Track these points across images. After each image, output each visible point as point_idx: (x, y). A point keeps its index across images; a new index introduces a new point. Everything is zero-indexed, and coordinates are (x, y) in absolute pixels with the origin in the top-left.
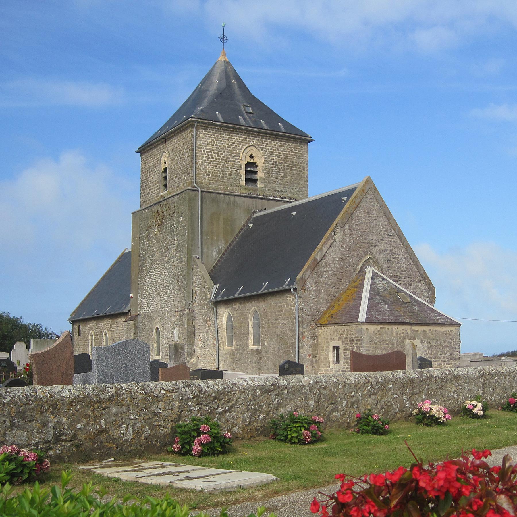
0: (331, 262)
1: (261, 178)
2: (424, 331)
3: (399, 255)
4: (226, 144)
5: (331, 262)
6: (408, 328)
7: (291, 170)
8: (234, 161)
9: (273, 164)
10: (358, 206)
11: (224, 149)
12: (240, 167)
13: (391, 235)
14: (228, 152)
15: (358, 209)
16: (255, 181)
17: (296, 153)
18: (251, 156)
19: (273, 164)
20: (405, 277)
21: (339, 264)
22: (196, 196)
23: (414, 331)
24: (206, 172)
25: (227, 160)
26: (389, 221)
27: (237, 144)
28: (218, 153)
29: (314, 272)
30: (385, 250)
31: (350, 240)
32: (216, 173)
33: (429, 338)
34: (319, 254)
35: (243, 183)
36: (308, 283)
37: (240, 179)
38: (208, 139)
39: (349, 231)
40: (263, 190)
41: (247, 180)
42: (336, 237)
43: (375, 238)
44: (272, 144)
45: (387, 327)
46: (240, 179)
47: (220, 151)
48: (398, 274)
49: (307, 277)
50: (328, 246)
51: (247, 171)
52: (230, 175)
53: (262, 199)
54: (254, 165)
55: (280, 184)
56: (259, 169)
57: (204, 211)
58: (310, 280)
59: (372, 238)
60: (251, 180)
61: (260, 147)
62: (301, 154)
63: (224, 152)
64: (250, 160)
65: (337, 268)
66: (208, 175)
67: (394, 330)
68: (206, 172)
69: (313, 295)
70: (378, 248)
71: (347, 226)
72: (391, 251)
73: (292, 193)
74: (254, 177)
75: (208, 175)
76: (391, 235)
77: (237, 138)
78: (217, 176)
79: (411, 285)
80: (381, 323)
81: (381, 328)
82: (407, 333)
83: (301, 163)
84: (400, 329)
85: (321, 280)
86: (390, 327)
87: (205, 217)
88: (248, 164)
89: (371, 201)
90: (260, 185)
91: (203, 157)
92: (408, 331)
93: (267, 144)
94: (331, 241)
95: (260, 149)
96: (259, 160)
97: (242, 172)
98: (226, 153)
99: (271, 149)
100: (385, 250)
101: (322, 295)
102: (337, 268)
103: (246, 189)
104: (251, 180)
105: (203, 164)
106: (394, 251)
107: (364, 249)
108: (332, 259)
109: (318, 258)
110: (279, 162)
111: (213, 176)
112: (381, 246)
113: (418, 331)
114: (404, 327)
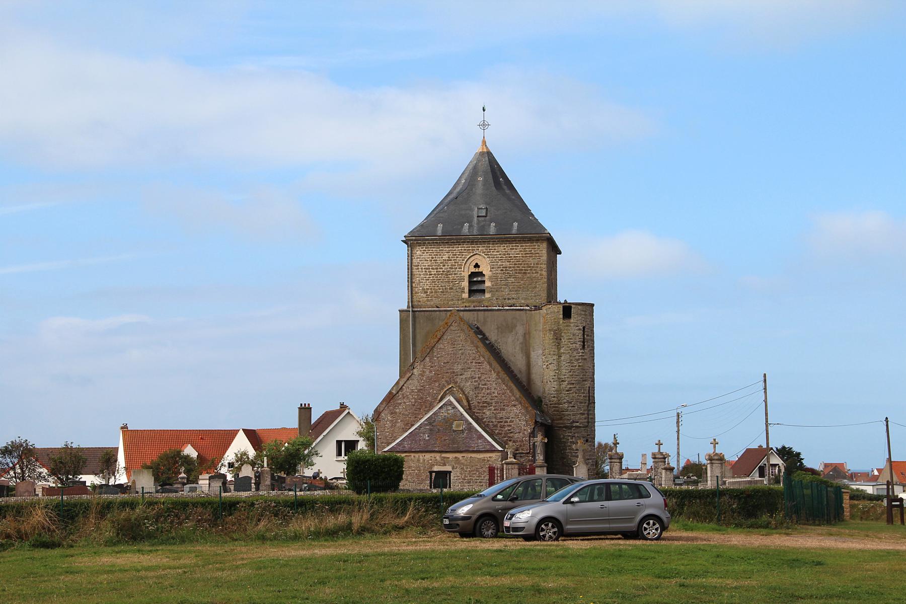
4: (446, 257)
6: (438, 456)
7: (525, 273)
11: (444, 263)
12: (462, 280)
18: (477, 266)
20: (496, 403)
22: (408, 316)
25: (447, 274)
31: (431, 372)
33: (463, 464)
35: (466, 295)
38: (426, 256)
40: (489, 300)
41: (471, 292)
42: (415, 370)
44: (500, 250)
45: (413, 455)
48: (488, 400)
51: (470, 282)
53: (484, 310)
54: (481, 274)
56: (486, 278)
57: (418, 331)
58: (386, 412)
59: (458, 368)
64: (474, 270)
69: (388, 424)
70: (464, 377)
71: (427, 359)
73: (525, 299)
74: (481, 287)
77: (458, 249)
79: (504, 410)
80: (405, 452)
84: (428, 456)
86: (417, 455)
87: (418, 337)
88: (473, 275)
90: (487, 295)
92: (438, 458)
94: (408, 375)
96: (485, 269)
97: (465, 284)
100: (472, 378)
101: (398, 425)
103: (470, 302)
106: (483, 378)
109: (394, 392)
112: (468, 374)
114: (433, 455)
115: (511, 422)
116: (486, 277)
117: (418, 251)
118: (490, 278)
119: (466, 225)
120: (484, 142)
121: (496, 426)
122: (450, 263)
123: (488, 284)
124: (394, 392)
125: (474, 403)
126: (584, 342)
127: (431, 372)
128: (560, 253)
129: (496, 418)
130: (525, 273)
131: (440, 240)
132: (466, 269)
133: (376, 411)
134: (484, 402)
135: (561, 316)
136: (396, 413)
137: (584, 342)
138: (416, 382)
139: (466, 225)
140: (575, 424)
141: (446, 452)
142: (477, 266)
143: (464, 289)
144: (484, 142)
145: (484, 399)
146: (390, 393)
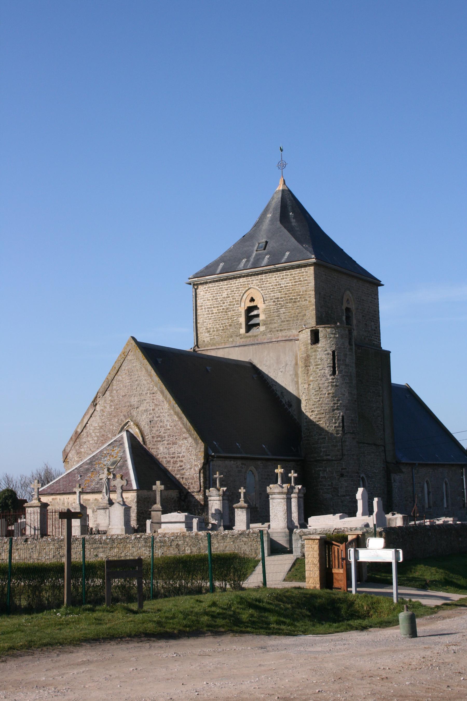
0: (91, 431)
1: (263, 320)
2: (96, 499)
3: (162, 413)
4: (225, 295)
5: (91, 431)
7: (295, 302)
8: (233, 311)
9: (274, 302)
12: (239, 315)
14: (227, 303)
15: (119, 373)
17: (300, 281)
18: (252, 300)
21: (100, 432)
24: (207, 329)
25: (226, 311)
26: (151, 378)
27: (236, 291)
28: (218, 307)
29: (76, 444)
30: (146, 411)
32: (216, 328)
34: (80, 426)
35: (243, 331)
36: (70, 455)
37: (241, 328)
38: (208, 295)
39: (110, 398)
41: (249, 328)
43: (136, 399)
45: (58, 497)
47: (219, 304)
49: (69, 449)
50: (88, 416)
52: (230, 325)
54: (256, 308)
55: (283, 322)
58: (73, 452)
59: (134, 401)
61: (260, 287)
62: (306, 280)
63: (224, 303)
65: (97, 437)
66: (209, 332)
67: (66, 500)
68: (207, 329)
71: (108, 393)
72: (153, 410)
75: (209, 332)
76: (153, 393)
78: (217, 331)
81: (53, 499)
83: (306, 291)
85: (82, 450)
88: (250, 309)
89: (133, 361)
90: (262, 328)
91: (204, 315)
93: (267, 281)
95: (260, 289)
97: (242, 320)
98: (226, 304)
99: (272, 286)
102: (97, 437)
105: (204, 322)
106: (157, 409)
107: (125, 413)
108: (93, 428)
110: (282, 298)
111: (214, 331)
113: (89, 500)
115: (184, 457)
118: (264, 310)
119: (244, 261)
122: (228, 300)
123: (262, 317)
124: (79, 430)
127: (111, 406)
129: (169, 454)
130: (295, 302)
132: (243, 304)
134: (159, 436)
135: (310, 341)
136: (81, 453)
138: (98, 418)
139: (244, 261)
140: (325, 458)
142: (252, 300)
143: (241, 324)
145: (157, 433)
146: (76, 432)
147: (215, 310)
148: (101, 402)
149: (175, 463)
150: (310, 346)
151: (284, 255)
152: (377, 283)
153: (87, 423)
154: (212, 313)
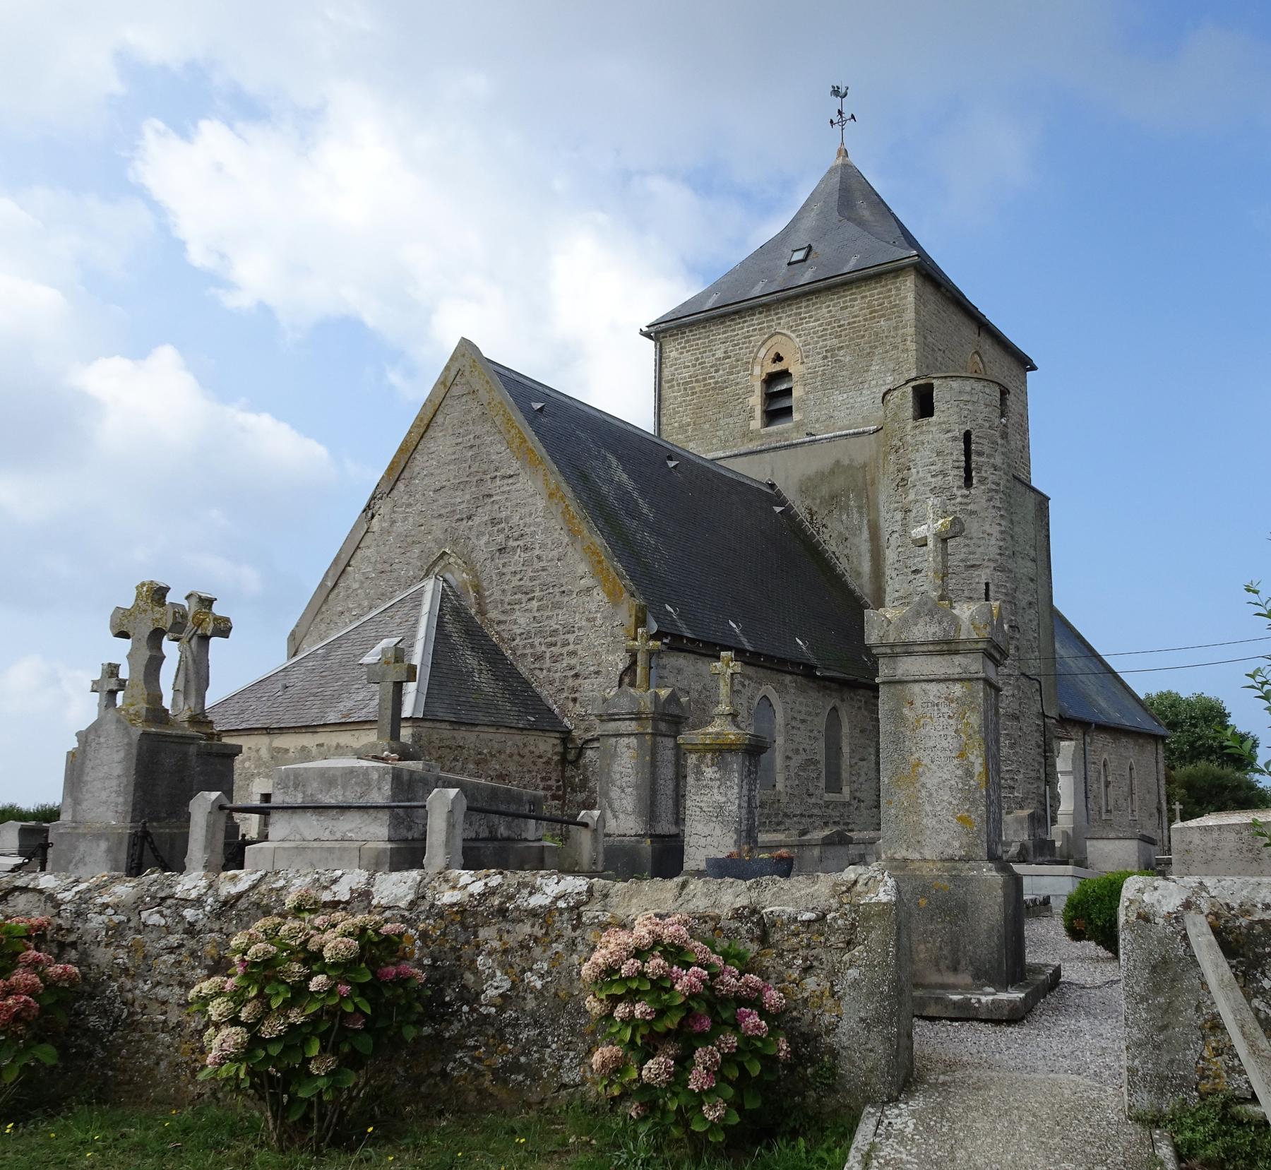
2: (304, 748)
4: (720, 354)
10: (428, 426)
13: (511, 476)
15: (430, 433)
16: (788, 412)
18: (778, 358)
19: (825, 358)
23: (279, 750)
28: (705, 379)
35: (756, 424)
37: (752, 417)
38: (687, 357)
40: (799, 425)
46: (752, 417)
54: (785, 374)
60: (776, 410)
61: (794, 331)
62: (895, 306)
63: (717, 371)
70: (477, 520)
76: (511, 476)
79: (558, 606)
82: (260, 758)
83: (896, 328)
88: (772, 379)
89: (464, 399)
90: (796, 416)
93: (811, 317)
95: (793, 335)
97: (756, 401)
104: (776, 410)
113: (287, 751)
116: (795, 378)
117: (672, 352)
120: (844, 153)
121: (539, 658)
125: (493, 593)
126: (968, 470)
128: (1034, 368)
131: (707, 320)
133: (293, 634)
137: (968, 470)
141: (282, 730)
142: (778, 358)
143: (752, 410)
144: (844, 153)
145: (515, 582)
147: (698, 387)
148: (384, 508)
149: (556, 659)
150: (910, 424)
151: (848, 261)
152: (1025, 364)
153: (348, 565)
154: (693, 394)
